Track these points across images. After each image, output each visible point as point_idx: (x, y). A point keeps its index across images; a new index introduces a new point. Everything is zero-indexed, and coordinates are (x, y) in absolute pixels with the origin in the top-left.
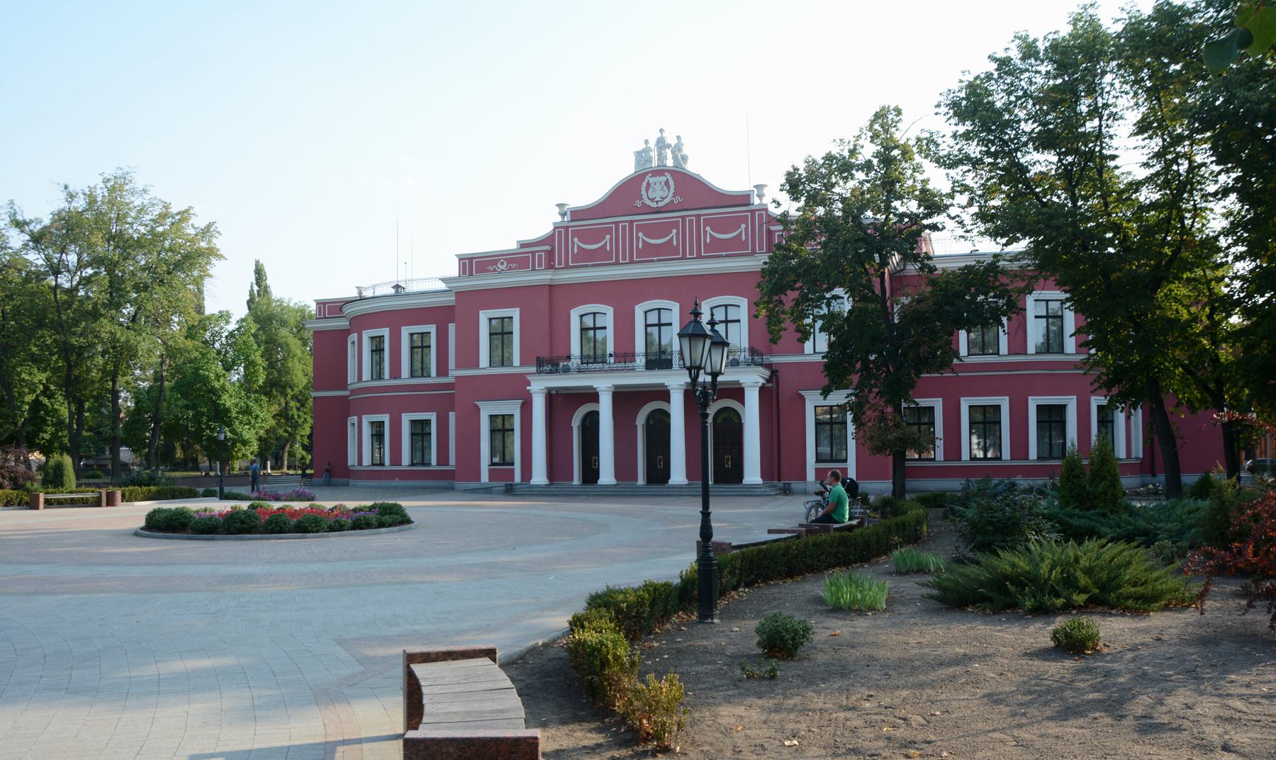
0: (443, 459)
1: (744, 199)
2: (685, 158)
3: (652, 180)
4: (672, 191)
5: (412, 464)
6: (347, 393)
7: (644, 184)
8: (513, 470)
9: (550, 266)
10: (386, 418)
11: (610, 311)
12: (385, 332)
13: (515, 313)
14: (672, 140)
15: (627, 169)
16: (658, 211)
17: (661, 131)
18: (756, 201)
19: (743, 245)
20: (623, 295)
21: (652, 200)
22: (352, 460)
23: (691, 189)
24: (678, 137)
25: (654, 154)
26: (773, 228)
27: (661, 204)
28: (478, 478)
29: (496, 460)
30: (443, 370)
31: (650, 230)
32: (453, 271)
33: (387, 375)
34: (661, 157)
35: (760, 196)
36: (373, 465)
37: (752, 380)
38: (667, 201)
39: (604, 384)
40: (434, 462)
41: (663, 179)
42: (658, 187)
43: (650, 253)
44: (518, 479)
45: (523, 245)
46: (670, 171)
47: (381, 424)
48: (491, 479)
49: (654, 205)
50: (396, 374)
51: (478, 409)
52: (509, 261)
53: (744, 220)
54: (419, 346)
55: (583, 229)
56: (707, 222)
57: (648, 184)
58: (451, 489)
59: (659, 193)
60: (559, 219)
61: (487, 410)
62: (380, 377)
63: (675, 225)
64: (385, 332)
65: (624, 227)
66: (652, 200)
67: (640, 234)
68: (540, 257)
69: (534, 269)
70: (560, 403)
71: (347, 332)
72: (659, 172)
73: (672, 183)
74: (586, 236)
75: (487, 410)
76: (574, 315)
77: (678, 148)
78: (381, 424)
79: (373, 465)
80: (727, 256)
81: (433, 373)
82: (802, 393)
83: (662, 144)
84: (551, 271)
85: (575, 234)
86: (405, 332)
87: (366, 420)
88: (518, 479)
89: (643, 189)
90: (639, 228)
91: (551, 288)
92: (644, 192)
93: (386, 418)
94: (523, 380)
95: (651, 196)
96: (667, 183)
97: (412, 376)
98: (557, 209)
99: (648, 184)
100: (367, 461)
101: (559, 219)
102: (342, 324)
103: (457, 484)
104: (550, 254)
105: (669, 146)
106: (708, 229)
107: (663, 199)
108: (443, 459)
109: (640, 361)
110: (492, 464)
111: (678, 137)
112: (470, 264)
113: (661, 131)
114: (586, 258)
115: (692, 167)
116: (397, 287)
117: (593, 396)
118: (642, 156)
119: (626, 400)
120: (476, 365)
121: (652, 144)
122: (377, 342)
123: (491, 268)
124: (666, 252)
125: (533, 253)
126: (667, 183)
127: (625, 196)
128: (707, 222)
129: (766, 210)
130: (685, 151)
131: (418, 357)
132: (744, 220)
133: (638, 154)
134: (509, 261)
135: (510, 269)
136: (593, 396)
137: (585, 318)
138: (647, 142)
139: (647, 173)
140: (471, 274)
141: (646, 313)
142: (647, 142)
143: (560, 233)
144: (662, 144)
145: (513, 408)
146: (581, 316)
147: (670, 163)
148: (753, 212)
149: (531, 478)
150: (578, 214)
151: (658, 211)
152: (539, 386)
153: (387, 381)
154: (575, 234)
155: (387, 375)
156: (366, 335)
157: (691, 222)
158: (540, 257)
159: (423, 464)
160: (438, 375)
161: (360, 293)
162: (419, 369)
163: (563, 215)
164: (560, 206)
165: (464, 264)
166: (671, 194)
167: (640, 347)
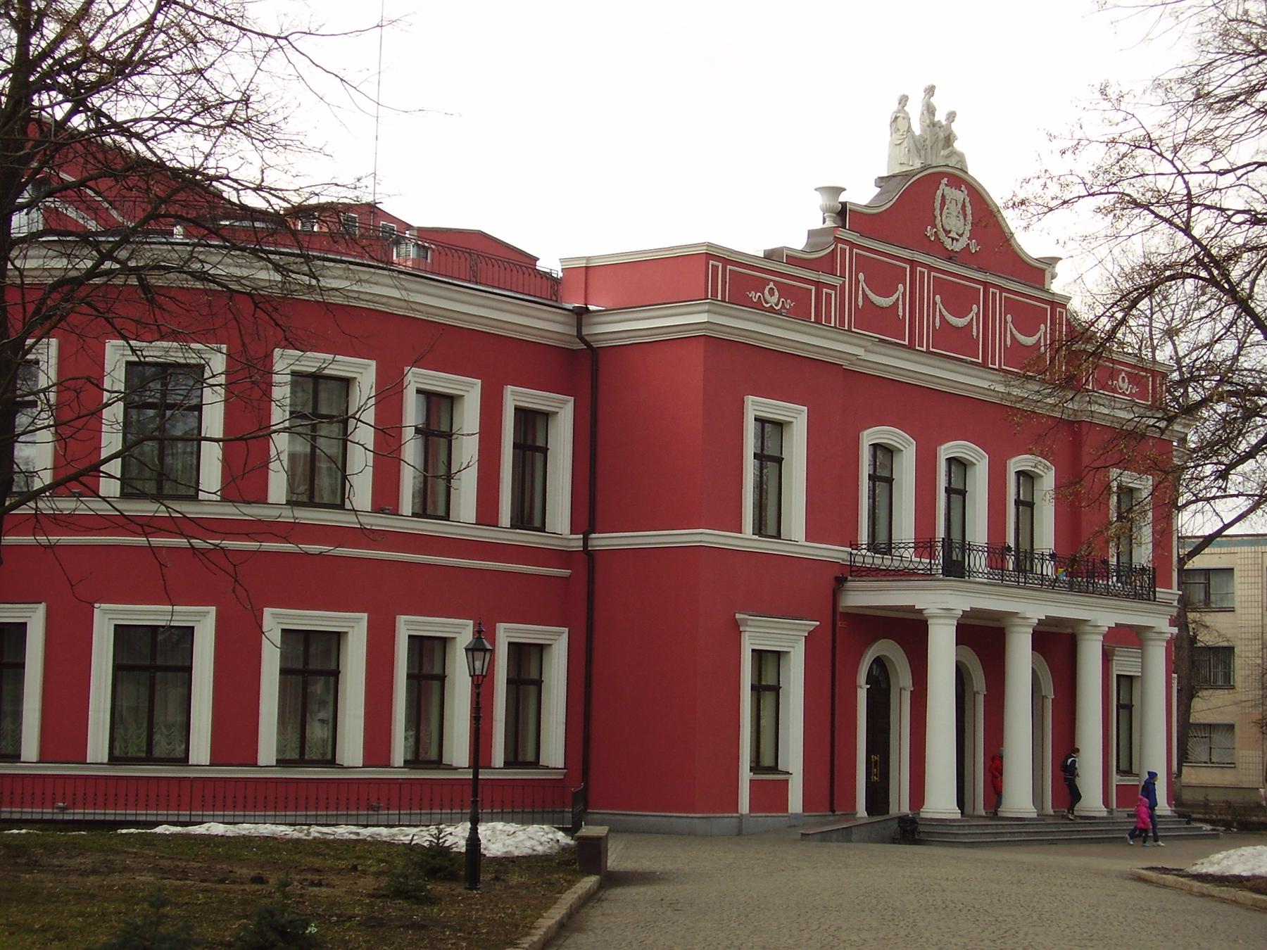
16: (950, 256)
17: (931, 90)
21: (948, 232)
24: (952, 116)
27: (958, 247)
49: (948, 244)
61: (757, 634)
75: (757, 634)
89: (937, 204)
92: (937, 212)
96: (964, 206)
126: (964, 206)
129: (1064, 306)
130: (958, 146)
151: (950, 256)
153: (405, 522)
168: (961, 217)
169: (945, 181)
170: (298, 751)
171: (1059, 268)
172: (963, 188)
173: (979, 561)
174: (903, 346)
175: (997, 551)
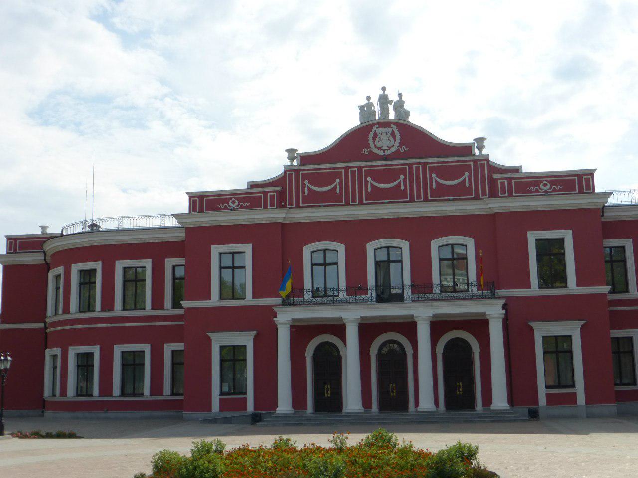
0: (157, 388)
1: (466, 150)
2: (407, 113)
3: (379, 131)
4: (398, 141)
5: (123, 394)
6: (41, 325)
7: (371, 134)
8: (244, 401)
9: (281, 205)
10: (96, 350)
11: (341, 248)
12: (98, 266)
13: (248, 248)
14: (393, 97)
15: (353, 121)
16: (386, 158)
17: (384, 89)
18: (477, 152)
19: (468, 191)
20: (355, 235)
21: (379, 149)
22: (47, 392)
23: (417, 141)
24: (400, 95)
25: (377, 108)
26: (495, 176)
27: (388, 153)
28: (210, 409)
29: (226, 389)
30: (158, 302)
31: (378, 175)
32: (184, 207)
33: (98, 306)
34: (384, 111)
35: (481, 148)
36: (78, 395)
37: (494, 311)
38: (394, 150)
39: (351, 316)
40: (147, 390)
41: (389, 130)
42: (385, 137)
43: (377, 196)
44: (250, 407)
45: (253, 185)
46: (395, 124)
47: (90, 355)
48: (221, 409)
49: (381, 153)
50: (108, 304)
51: (209, 340)
52: (240, 200)
53: (467, 168)
54: (133, 280)
55: (311, 175)
56: (432, 170)
57: (375, 135)
58: (180, 419)
59: (386, 143)
60: (288, 163)
61: (219, 340)
62: (90, 308)
63: (403, 171)
64: (98, 266)
65: (353, 172)
66: (379, 149)
67: (369, 179)
68: (272, 197)
69: (266, 207)
70: (301, 332)
71: (48, 267)
72: (385, 124)
73: (397, 134)
74: (316, 179)
75: (219, 340)
76: (307, 250)
77: (399, 105)
78: (90, 355)
79: (78, 395)
80: (454, 200)
81: (148, 304)
82: (531, 324)
83: (384, 100)
84: (284, 210)
85: (305, 177)
86: (120, 265)
87: (73, 351)
88: (250, 407)
90: (368, 173)
91: (284, 227)
93: (96, 350)
94: (270, 312)
95: (378, 145)
97: (124, 309)
98: (286, 155)
99: (375, 135)
100: (71, 391)
101: (288, 163)
102: (35, 258)
103: (185, 414)
104: (281, 194)
105: (391, 102)
106: (434, 175)
107: (390, 148)
108: (157, 388)
109: (372, 294)
110: (222, 393)
111: (400, 95)
112: (201, 202)
113: (384, 89)
114: (314, 199)
115: (415, 120)
116: (93, 225)
117: (339, 329)
118: (366, 110)
119: (368, 330)
120: (208, 297)
121: (375, 100)
122: (87, 278)
123: (222, 206)
124: (395, 195)
125: (265, 193)
127: (353, 144)
128: (432, 170)
129: (488, 160)
130: (407, 106)
131: (130, 292)
132: (467, 168)
133: (362, 108)
134: (240, 200)
135: (242, 207)
136: (339, 329)
137: (314, 255)
138: (369, 98)
139: (374, 125)
140: (201, 210)
141: (375, 250)
142: (369, 98)
143: (290, 176)
144: (384, 100)
145: (246, 339)
146: (312, 253)
147: (392, 115)
148: (475, 162)
149: (275, 406)
150: (306, 159)
152: (284, 318)
153: (98, 312)
154: (305, 177)
155: (98, 306)
156: (75, 268)
157: (418, 169)
158: (272, 197)
159: (134, 395)
160: (153, 308)
161: (62, 231)
162: (133, 300)
163: (291, 159)
164: (291, 152)
165: (195, 202)
166: (397, 144)
167: (371, 281)
168: (392, 139)
169: (377, 126)
170: (84, 390)
171: (485, 143)
172: (392, 126)
173: (408, 293)
174: (343, 205)
175: (415, 288)
